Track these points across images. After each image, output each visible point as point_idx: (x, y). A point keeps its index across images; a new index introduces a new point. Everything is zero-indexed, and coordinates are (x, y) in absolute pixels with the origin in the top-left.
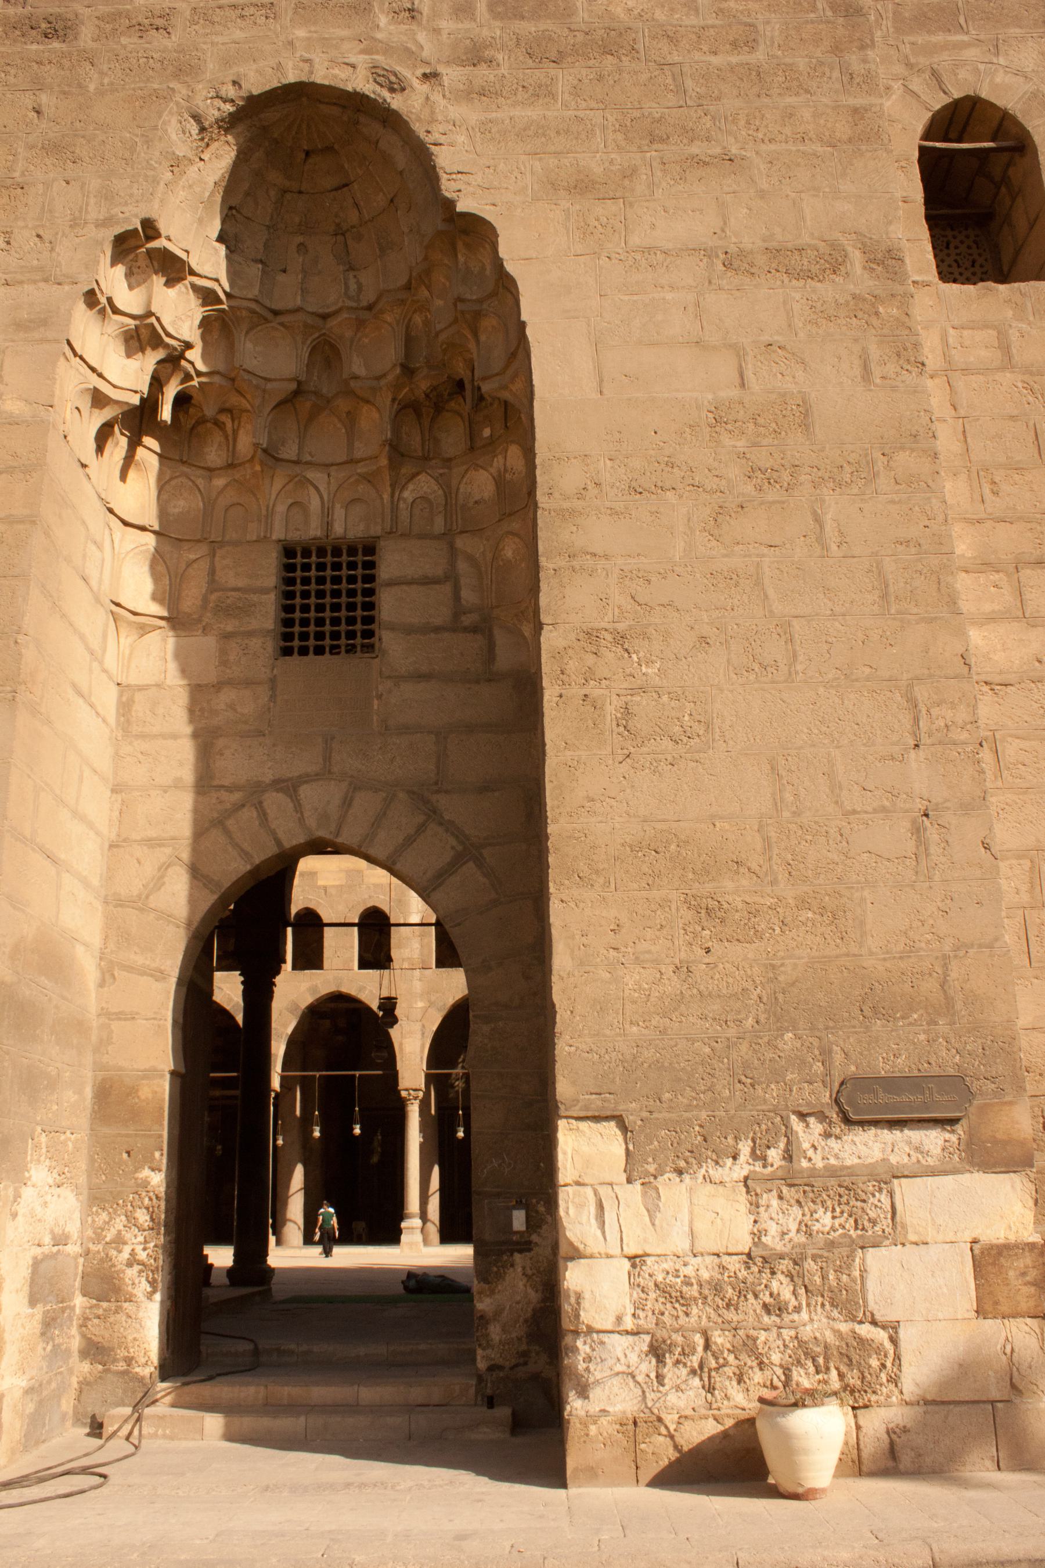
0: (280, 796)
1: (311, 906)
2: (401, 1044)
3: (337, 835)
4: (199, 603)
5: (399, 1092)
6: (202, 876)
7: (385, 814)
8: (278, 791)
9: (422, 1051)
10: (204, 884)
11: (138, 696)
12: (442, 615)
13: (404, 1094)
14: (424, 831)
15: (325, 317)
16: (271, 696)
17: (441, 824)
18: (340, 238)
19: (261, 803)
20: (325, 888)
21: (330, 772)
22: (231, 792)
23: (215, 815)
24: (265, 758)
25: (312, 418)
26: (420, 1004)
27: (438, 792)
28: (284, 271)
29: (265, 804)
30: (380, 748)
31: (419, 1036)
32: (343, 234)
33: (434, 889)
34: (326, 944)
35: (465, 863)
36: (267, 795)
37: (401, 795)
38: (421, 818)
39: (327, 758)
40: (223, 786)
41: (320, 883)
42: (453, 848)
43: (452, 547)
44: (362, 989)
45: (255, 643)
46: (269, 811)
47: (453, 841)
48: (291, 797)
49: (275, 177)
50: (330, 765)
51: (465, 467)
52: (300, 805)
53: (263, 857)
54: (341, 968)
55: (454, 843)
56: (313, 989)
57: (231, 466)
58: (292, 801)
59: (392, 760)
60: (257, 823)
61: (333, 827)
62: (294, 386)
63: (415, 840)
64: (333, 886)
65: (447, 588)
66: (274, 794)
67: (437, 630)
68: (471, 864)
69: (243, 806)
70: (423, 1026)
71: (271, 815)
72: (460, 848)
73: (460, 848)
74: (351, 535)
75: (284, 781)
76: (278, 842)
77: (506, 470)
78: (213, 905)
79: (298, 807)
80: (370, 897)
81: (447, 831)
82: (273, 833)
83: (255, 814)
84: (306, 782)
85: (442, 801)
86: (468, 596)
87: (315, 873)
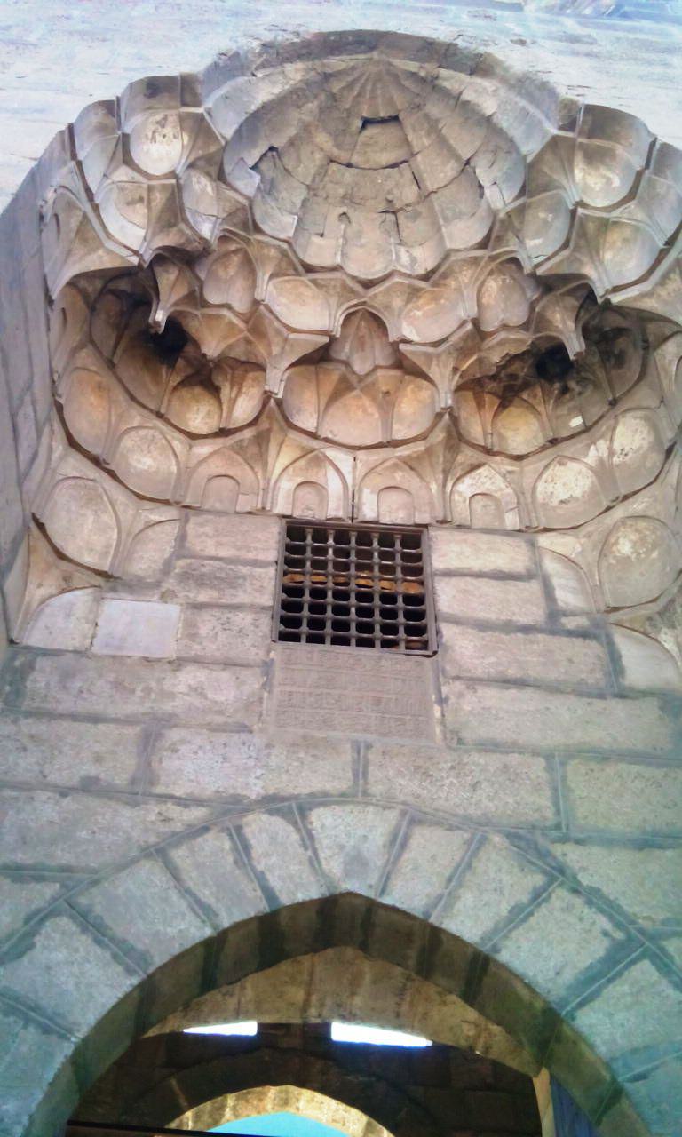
0: (278, 824)
3: (383, 891)
4: (158, 566)
6: (112, 939)
7: (469, 866)
8: (271, 812)
10: (115, 957)
11: (41, 663)
12: (534, 613)
14: (546, 900)
15: (368, 284)
16: (264, 685)
17: (575, 891)
18: (391, 217)
19: (239, 829)
21: (365, 793)
22: (186, 806)
23: (153, 839)
24: (251, 762)
25: (335, 396)
27: (564, 840)
28: (322, 235)
29: (247, 831)
30: (452, 768)
32: (394, 213)
33: (581, 1005)
35: (633, 962)
36: (250, 817)
37: (497, 839)
38: (538, 880)
39: (360, 771)
40: (172, 797)
42: (606, 934)
43: (532, 544)
45: (244, 619)
46: (253, 842)
47: (604, 923)
48: (295, 824)
49: (323, 139)
50: (366, 783)
51: (544, 463)
52: (311, 837)
53: (239, 916)
55: (608, 926)
57: (223, 433)
58: (298, 830)
59: (475, 786)
60: (230, 859)
61: (374, 878)
62: (326, 340)
63: (531, 914)
65: (535, 587)
66: (265, 817)
67: (526, 629)
68: (646, 964)
69: (206, 829)
71: (257, 851)
72: (619, 935)
73: (619, 935)
74: (387, 519)
75: (283, 799)
76: (269, 894)
77: (612, 453)
78: (127, 996)
79: (309, 840)
81: (589, 903)
82: (260, 878)
83: (227, 845)
84: (324, 804)
85: (572, 856)
86: (566, 597)
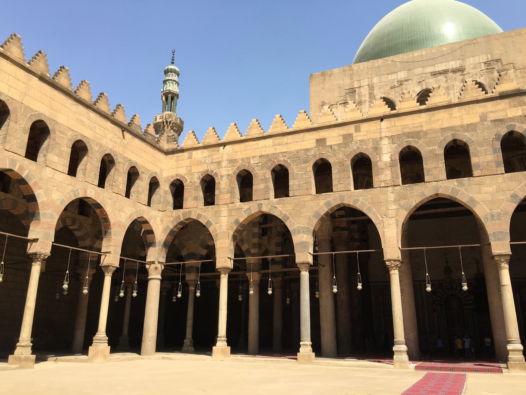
1: (324, 157)
2: (384, 232)
5: (384, 262)
9: (397, 236)
13: (387, 263)
20: (331, 146)
26: (394, 207)
31: (395, 226)
34: (333, 177)
41: (328, 144)
44: (356, 201)
54: (344, 191)
56: (327, 204)
64: (336, 145)
70: (397, 220)
80: (358, 148)
87: (325, 139)
